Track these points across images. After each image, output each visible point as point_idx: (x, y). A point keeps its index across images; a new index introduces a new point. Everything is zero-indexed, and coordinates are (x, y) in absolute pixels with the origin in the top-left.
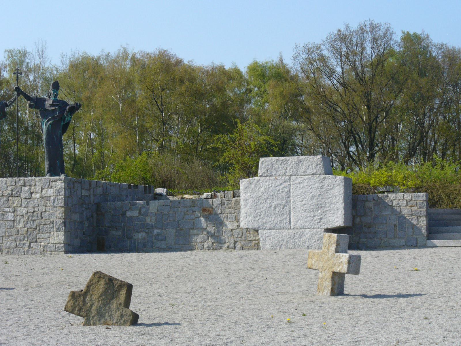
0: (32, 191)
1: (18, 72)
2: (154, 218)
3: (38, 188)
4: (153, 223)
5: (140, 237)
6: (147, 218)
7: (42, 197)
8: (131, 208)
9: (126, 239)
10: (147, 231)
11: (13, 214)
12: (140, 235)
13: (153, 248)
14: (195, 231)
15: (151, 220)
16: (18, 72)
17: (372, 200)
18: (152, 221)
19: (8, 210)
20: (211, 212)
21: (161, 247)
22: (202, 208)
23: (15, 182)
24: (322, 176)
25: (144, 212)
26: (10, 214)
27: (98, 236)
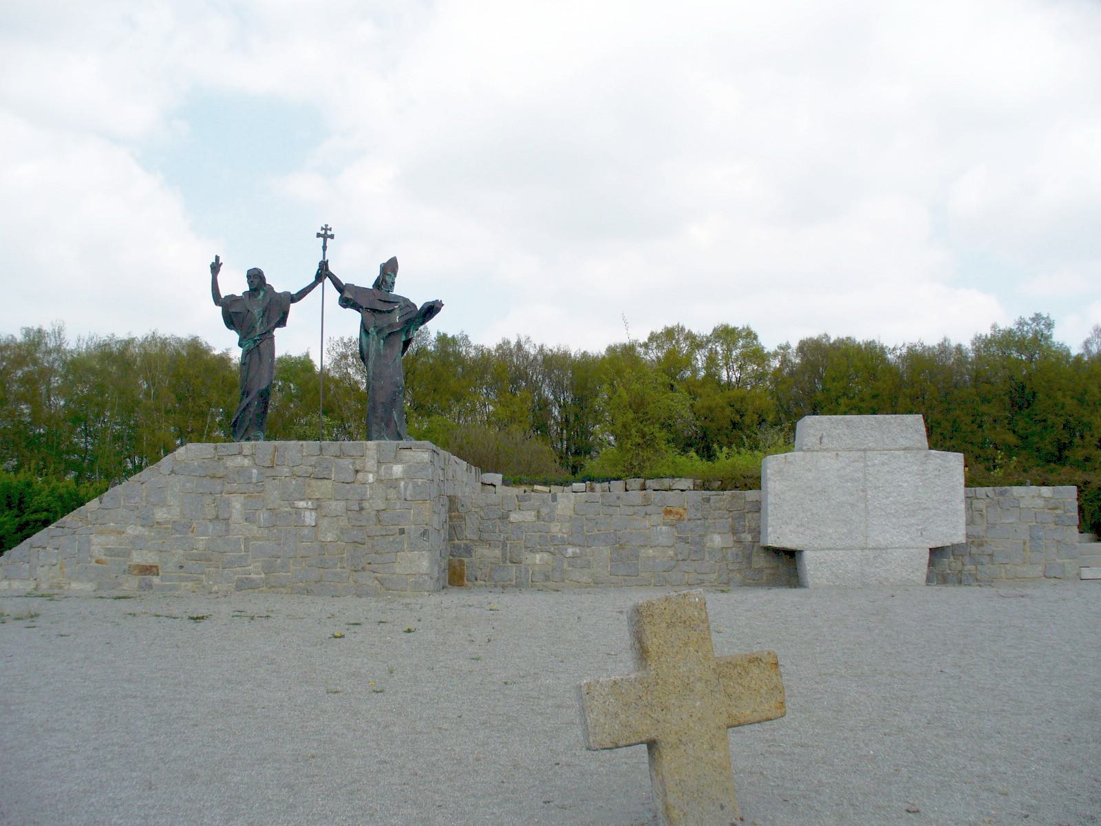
0: (358, 468)
1: (326, 233)
2: (567, 524)
3: (371, 463)
4: (565, 536)
5: (537, 562)
6: (552, 525)
7: (379, 480)
8: (519, 506)
9: (509, 564)
10: (552, 549)
11: (313, 513)
12: (538, 556)
13: (563, 581)
14: (651, 551)
15: (560, 530)
16: (326, 233)
17: (984, 497)
18: (564, 531)
19: (302, 504)
20: (681, 515)
21: (580, 580)
22: (663, 509)
23: (321, 449)
24: (923, 453)
25: (546, 515)
26: (307, 513)
27: (451, 558)
